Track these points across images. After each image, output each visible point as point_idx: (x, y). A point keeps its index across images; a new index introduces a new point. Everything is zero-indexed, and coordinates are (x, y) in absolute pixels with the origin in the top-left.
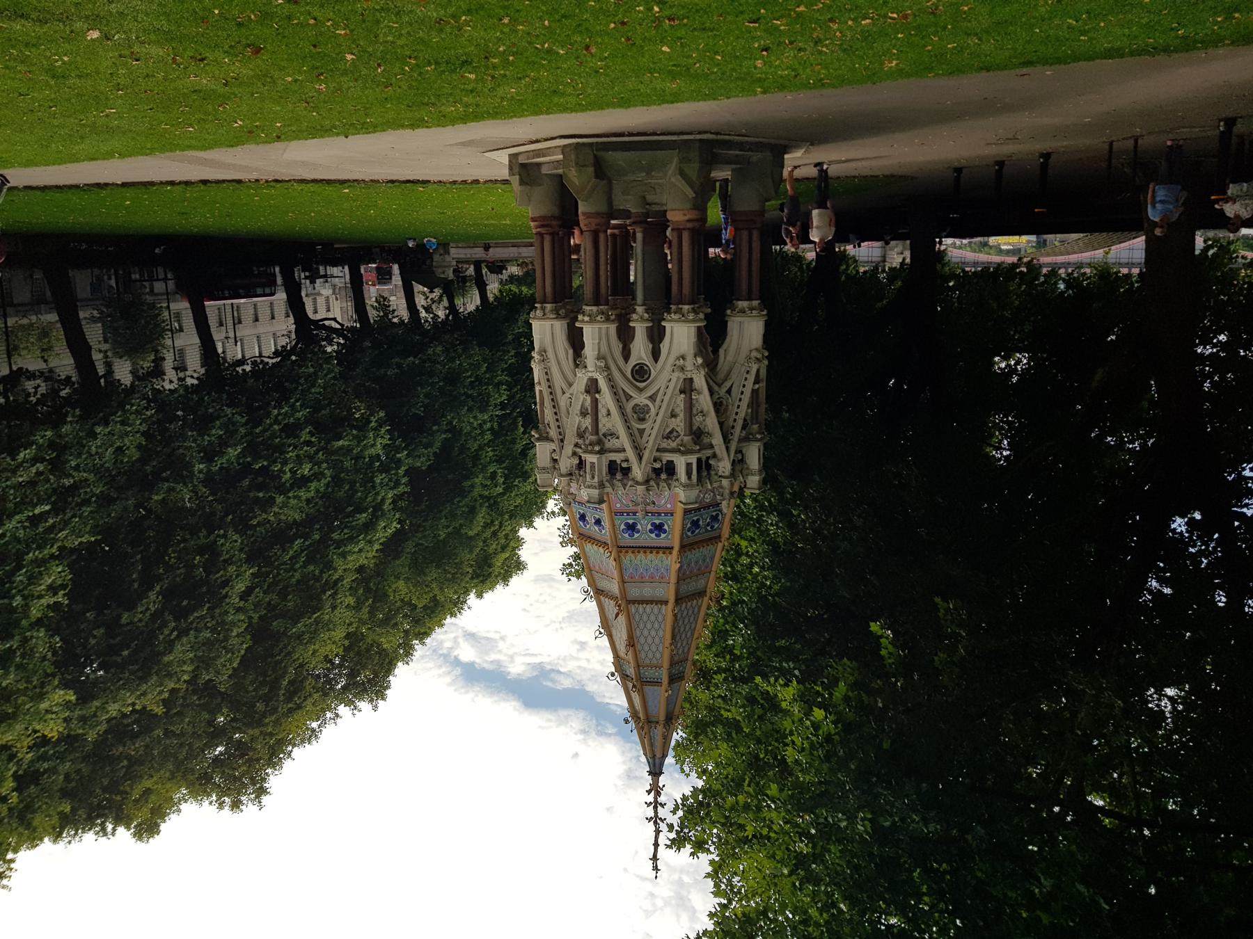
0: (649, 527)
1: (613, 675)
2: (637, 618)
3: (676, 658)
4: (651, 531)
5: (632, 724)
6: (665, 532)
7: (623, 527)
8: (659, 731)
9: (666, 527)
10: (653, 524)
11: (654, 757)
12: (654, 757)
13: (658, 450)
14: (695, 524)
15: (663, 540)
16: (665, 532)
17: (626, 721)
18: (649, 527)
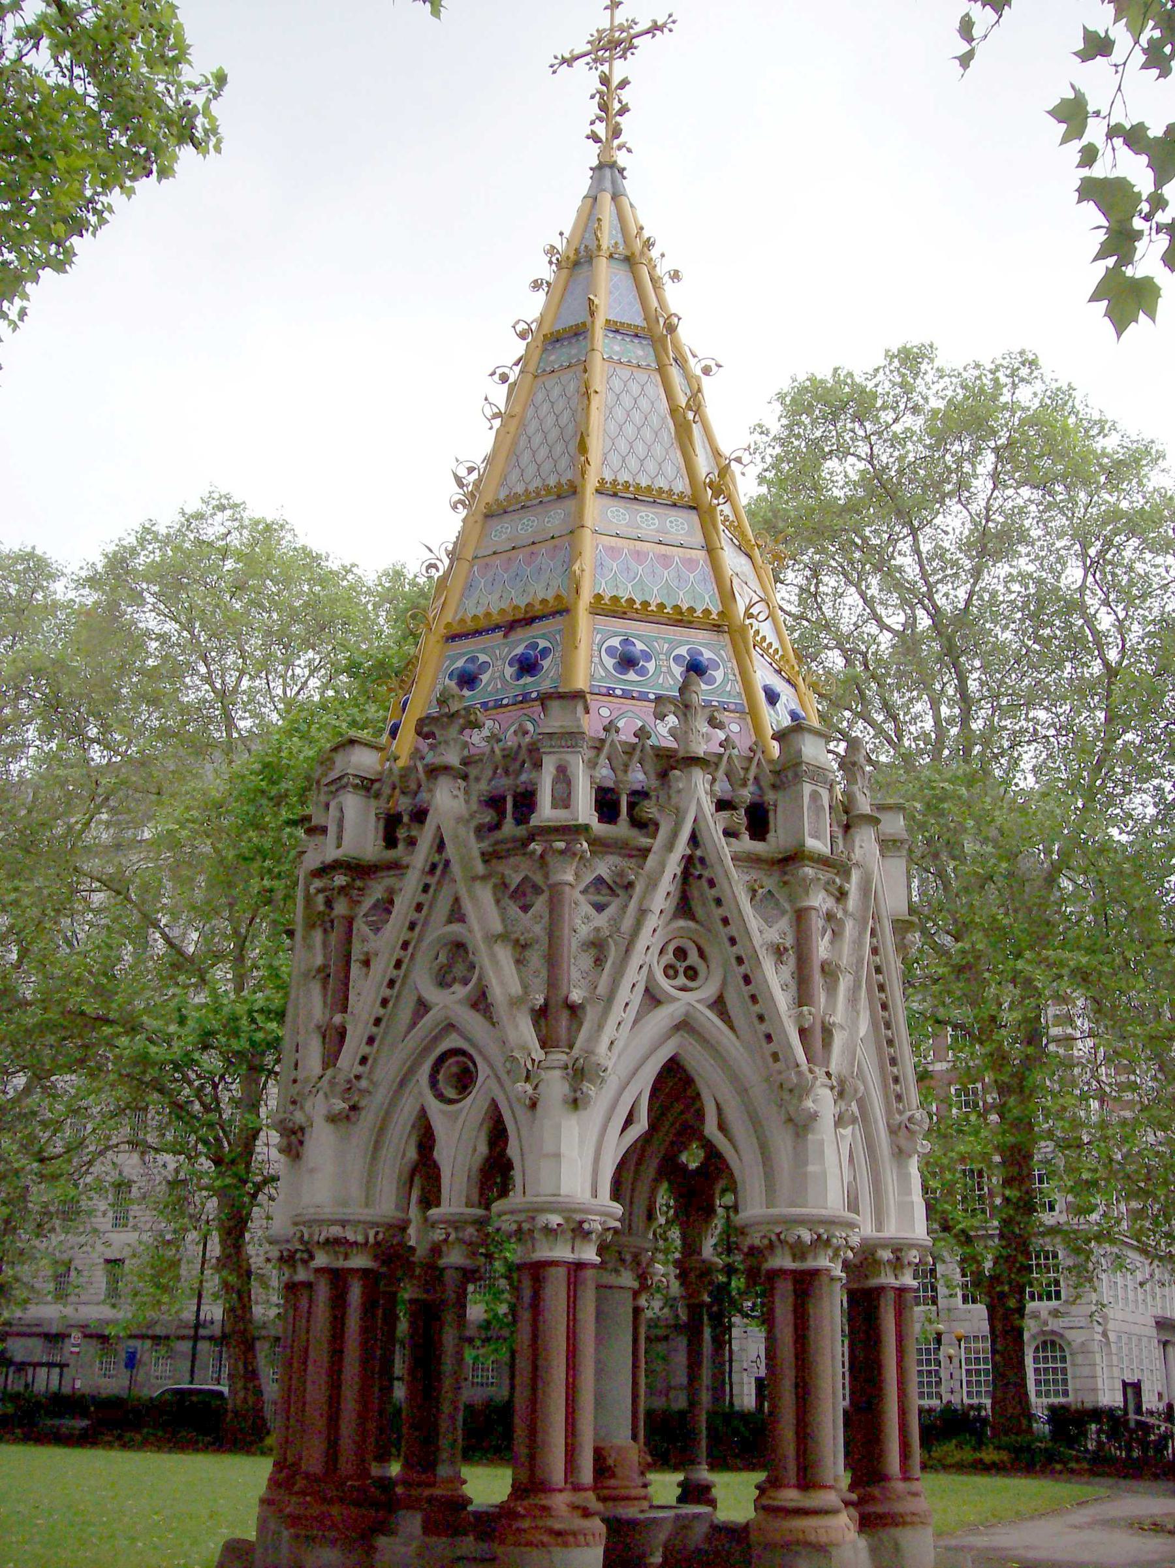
0: (651, 666)
1: (707, 371)
2: (669, 469)
3: (566, 376)
4: (647, 657)
5: (662, 269)
6: (611, 651)
7: (719, 675)
8: (608, 237)
9: (610, 662)
10: (642, 672)
11: (615, 197)
12: (615, 197)
13: (645, 852)
14: (527, 666)
15: (614, 633)
16: (611, 651)
17: (675, 276)
18: (651, 666)
